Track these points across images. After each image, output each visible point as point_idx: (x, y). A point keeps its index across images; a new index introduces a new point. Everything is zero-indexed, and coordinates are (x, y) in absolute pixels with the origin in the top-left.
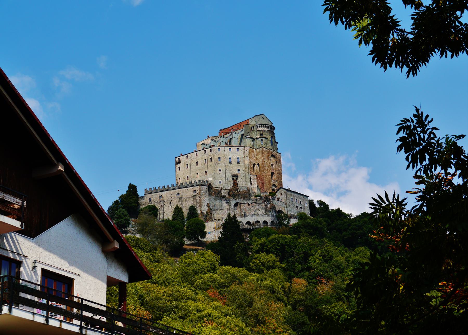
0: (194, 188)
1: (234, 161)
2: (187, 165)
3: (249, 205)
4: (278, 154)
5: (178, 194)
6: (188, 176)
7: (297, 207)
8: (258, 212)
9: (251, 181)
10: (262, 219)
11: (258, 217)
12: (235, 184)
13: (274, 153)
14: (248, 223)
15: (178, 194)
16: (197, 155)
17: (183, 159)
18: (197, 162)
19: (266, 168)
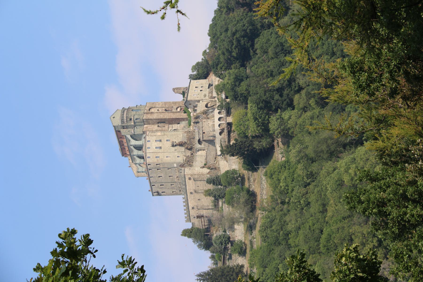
0: (187, 179)
1: (159, 144)
2: (161, 185)
3: (204, 133)
4: (147, 105)
5: (191, 193)
6: (171, 185)
7: (201, 91)
8: (210, 125)
9: (174, 130)
10: (217, 123)
11: (215, 125)
13: (148, 109)
14: (221, 133)
17: (155, 189)
18: (159, 177)
19: (162, 116)
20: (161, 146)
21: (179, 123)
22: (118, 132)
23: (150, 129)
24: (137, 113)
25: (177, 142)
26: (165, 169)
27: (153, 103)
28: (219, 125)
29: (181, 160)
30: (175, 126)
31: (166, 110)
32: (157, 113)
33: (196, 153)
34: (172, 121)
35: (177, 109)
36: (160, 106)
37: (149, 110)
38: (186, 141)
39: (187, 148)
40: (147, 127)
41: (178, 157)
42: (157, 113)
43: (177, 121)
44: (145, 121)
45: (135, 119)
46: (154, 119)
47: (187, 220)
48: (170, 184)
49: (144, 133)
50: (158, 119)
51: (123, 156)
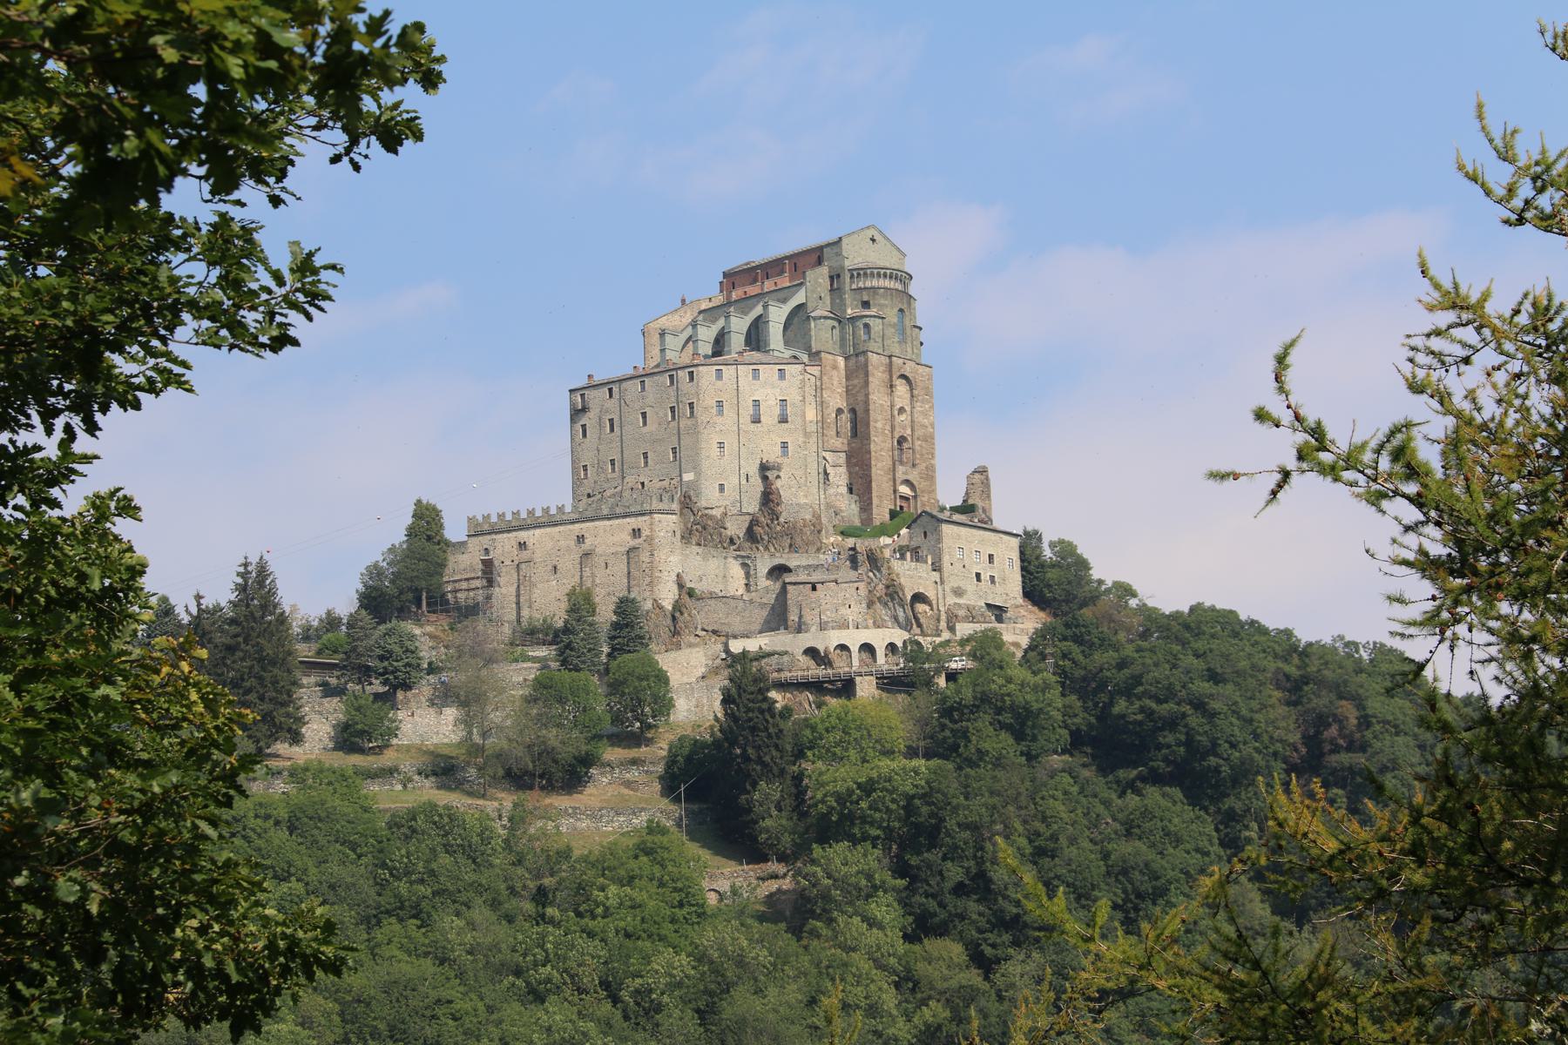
0: (633, 522)
1: (770, 414)
2: (611, 420)
3: (814, 589)
4: (921, 369)
5: (581, 539)
6: (612, 462)
7: (978, 575)
8: (844, 611)
9: (826, 474)
10: (854, 639)
11: (844, 632)
12: (769, 498)
13: (908, 369)
14: (811, 652)
16: (643, 389)
17: (597, 398)
18: (644, 415)
19: (879, 425)
20: (763, 421)
21: (851, 491)
22: (816, 256)
23: (831, 378)
24: (890, 331)
25: (778, 483)
26: (675, 439)
27: (928, 392)
28: (843, 647)
29: (710, 498)
30: (839, 477)
32: (892, 406)
33: (736, 558)
35: (907, 482)
36: (919, 418)
37: (903, 377)
38: (782, 520)
39: (754, 522)
40: (835, 367)
41: (721, 485)
42: (892, 406)
43: (860, 485)
44: (862, 358)
45: (867, 320)
46: (867, 395)
47: (478, 524)
48: (617, 457)
49: (815, 356)
50: (867, 411)
51: (725, 275)
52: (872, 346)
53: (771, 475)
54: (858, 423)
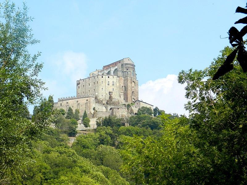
0: (87, 99)
1: (111, 84)
3: (118, 109)
5: (77, 101)
9: (120, 96)
12: (110, 97)
15: (77, 101)
20: (111, 85)
22: (119, 62)
27: (138, 85)
29: (100, 97)
30: (122, 97)
31: (133, 92)
34: (126, 95)
35: (134, 99)
36: (136, 89)
37: (133, 81)
39: (108, 101)
40: (122, 79)
43: (126, 99)
44: (127, 78)
49: (118, 77)
51: (104, 66)
52: (128, 76)
53: (111, 94)
54: (126, 88)
